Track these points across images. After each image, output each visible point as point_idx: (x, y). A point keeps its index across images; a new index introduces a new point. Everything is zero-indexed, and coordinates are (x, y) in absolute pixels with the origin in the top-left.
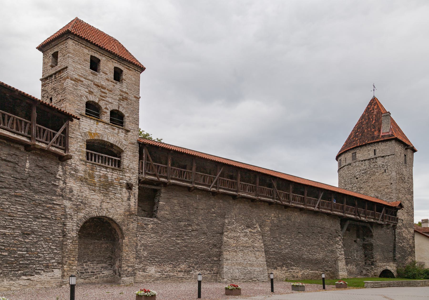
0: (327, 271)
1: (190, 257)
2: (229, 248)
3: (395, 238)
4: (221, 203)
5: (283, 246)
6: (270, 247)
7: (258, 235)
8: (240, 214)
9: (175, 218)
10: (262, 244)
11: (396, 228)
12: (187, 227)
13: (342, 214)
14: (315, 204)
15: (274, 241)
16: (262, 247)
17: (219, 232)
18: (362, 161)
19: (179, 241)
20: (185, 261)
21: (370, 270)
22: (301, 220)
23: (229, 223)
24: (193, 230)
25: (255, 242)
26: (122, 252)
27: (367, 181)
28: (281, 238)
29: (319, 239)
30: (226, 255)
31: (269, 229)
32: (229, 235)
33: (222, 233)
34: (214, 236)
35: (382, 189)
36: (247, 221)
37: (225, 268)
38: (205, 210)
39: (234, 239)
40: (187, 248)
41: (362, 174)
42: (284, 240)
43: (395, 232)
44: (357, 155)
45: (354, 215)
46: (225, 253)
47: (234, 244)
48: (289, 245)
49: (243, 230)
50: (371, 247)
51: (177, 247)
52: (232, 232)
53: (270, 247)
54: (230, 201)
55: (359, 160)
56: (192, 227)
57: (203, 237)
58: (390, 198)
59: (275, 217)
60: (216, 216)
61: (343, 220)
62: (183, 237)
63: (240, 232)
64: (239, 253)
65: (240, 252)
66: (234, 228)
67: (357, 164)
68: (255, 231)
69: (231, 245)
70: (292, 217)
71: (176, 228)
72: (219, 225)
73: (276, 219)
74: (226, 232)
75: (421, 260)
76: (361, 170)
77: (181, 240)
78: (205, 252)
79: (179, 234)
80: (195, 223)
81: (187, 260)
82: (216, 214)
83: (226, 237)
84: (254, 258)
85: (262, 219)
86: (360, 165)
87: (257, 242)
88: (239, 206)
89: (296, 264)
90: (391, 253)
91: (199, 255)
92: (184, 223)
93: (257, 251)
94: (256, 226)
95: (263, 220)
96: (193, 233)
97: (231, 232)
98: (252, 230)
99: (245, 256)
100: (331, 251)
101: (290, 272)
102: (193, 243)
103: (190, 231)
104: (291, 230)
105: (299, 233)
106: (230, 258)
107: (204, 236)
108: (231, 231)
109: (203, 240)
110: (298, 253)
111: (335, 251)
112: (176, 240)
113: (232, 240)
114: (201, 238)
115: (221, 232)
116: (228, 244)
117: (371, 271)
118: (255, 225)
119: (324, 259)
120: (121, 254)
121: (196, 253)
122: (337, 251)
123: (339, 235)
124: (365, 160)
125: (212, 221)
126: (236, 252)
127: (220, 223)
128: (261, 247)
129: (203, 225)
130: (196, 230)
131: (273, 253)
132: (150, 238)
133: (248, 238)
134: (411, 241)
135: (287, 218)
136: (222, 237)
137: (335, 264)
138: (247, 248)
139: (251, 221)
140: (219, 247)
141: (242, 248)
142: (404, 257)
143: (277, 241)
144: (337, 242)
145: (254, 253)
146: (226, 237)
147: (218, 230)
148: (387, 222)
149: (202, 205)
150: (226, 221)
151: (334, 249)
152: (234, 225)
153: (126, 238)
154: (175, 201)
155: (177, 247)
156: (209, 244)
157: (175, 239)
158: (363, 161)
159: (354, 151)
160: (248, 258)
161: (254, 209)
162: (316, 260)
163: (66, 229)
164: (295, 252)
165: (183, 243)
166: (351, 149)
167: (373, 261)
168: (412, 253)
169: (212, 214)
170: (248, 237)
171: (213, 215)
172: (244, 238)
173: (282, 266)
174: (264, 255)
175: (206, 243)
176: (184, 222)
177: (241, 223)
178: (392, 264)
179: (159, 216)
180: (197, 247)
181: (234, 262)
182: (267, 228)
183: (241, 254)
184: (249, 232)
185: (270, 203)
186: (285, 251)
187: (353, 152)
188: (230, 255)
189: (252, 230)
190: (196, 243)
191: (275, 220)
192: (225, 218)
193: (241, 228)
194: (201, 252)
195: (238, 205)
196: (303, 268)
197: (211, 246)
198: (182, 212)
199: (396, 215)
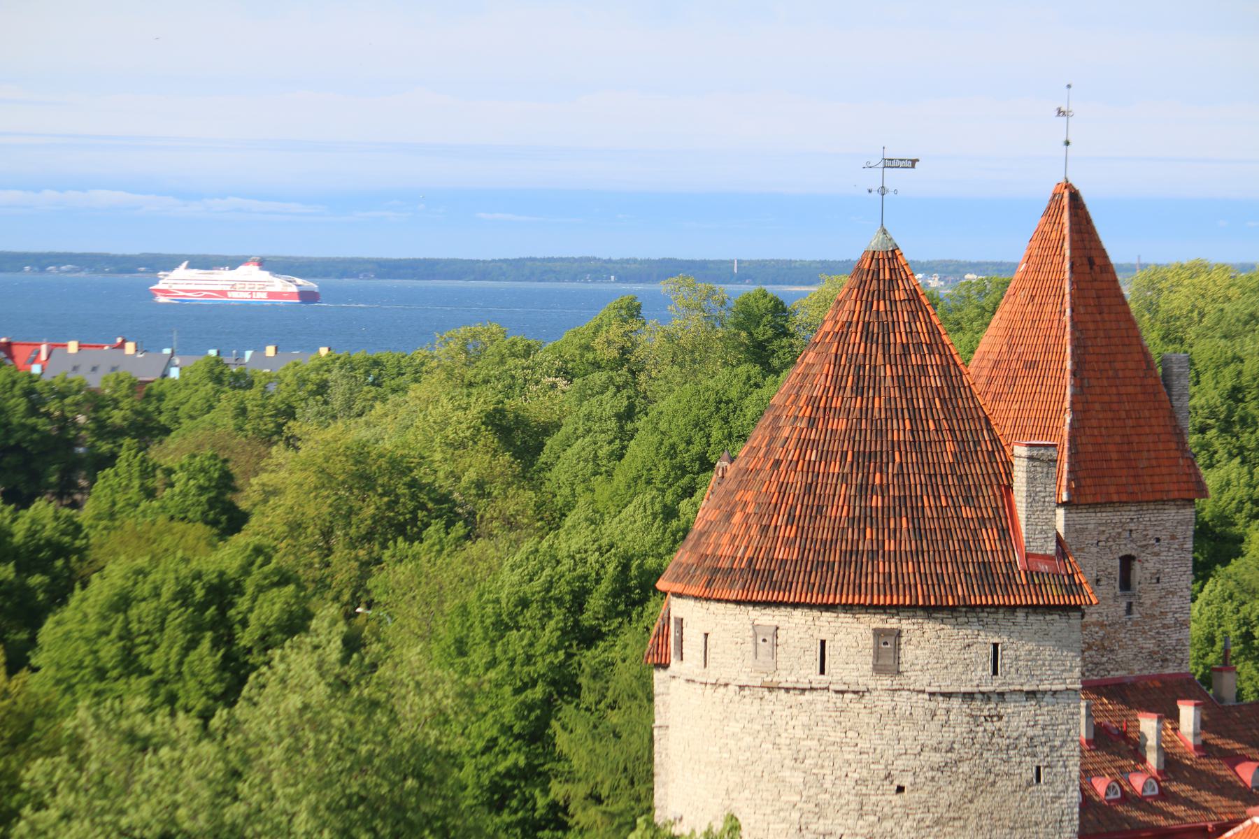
18: (932, 694)
27: (954, 819)
41: (932, 769)
44: (909, 653)
55: (918, 687)
86: (918, 713)
124: (948, 695)
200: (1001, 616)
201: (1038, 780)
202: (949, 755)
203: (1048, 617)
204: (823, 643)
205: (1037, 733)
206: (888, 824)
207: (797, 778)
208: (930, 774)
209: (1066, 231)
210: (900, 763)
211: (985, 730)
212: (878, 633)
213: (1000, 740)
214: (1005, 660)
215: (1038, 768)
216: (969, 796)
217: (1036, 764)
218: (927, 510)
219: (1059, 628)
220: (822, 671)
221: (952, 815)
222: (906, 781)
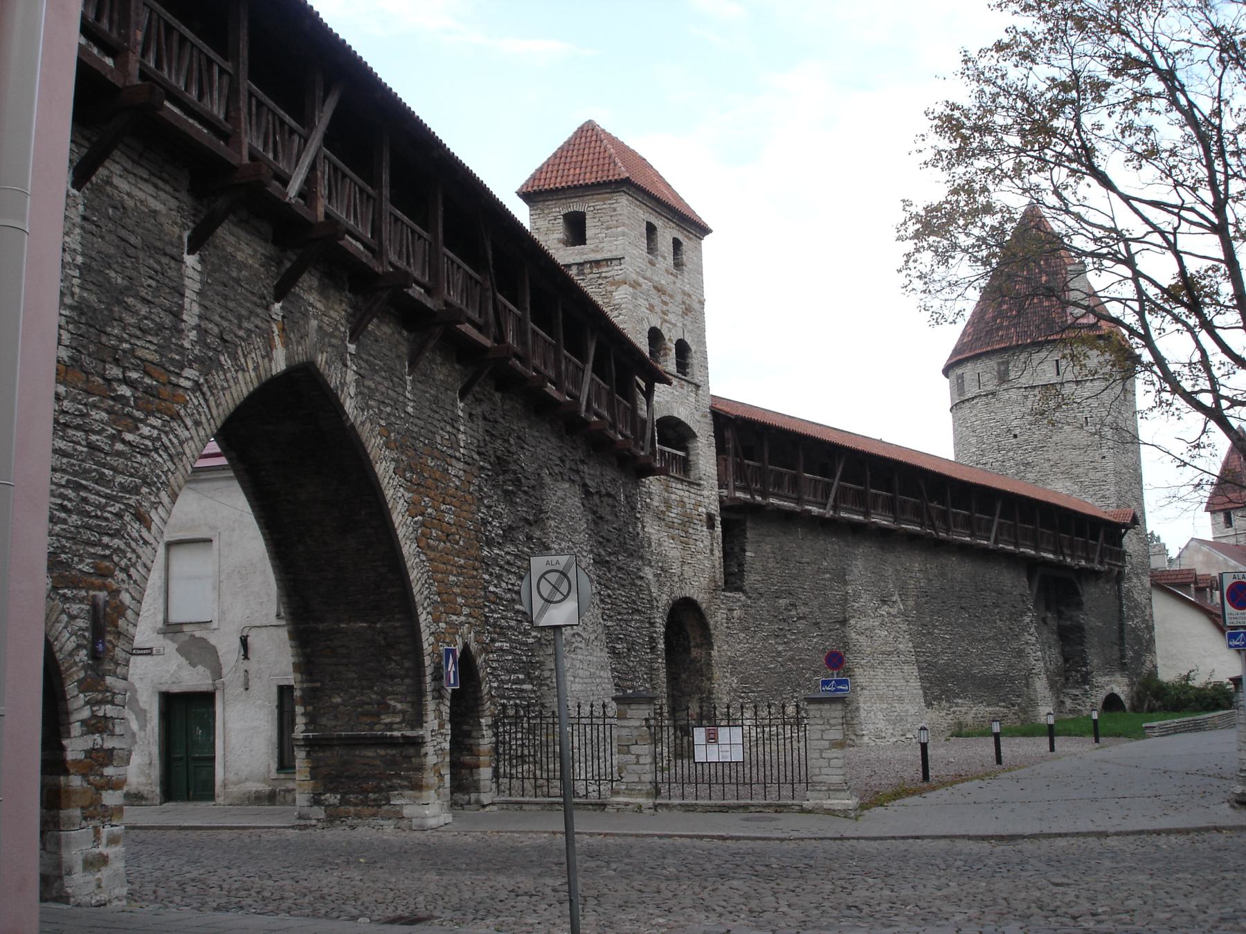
0: (1013, 705)
1: (799, 685)
3: (1121, 605)
4: (832, 545)
10: (911, 645)
11: (1122, 579)
12: (790, 610)
13: (1033, 552)
14: (989, 530)
15: (924, 635)
18: (1026, 388)
19: (780, 648)
20: (793, 697)
21: (1080, 696)
24: (799, 618)
26: (710, 679)
28: (934, 626)
30: (861, 676)
33: (844, 622)
35: (1081, 470)
37: (862, 710)
43: (1119, 590)
45: (1054, 553)
49: (876, 608)
58: (1103, 497)
59: (921, 570)
60: (830, 580)
61: (1031, 566)
68: (894, 611)
73: (922, 576)
81: (795, 695)
89: (962, 692)
90: (1116, 648)
94: (894, 599)
100: (1017, 653)
101: (954, 712)
102: (803, 649)
105: (962, 608)
115: (841, 617)
117: (1084, 699)
119: (1006, 674)
120: (706, 684)
122: (1028, 650)
123: (1029, 609)
126: (872, 667)
132: (739, 644)
134: (1147, 612)
137: (1027, 686)
142: (1138, 657)
144: (1025, 629)
148: (1109, 564)
150: (850, 589)
153: (715, 648)
154: (768, 548)
162: (994, 677)
163: (655, 632)
166: (994, 352)
167: (1087, 673)
168: (1147, 645)
169: (824, 573)
173: (938, 698)
178: (1118, 677)
179: (747, 588)
181: (873, 692)
182: (911, 603)
185: (911, 538)
192: (845, 583)
196: (977, 700)
199: (1121, 545)
206: (1011, 454)
207: (973, 440)
222: (1017, 431)
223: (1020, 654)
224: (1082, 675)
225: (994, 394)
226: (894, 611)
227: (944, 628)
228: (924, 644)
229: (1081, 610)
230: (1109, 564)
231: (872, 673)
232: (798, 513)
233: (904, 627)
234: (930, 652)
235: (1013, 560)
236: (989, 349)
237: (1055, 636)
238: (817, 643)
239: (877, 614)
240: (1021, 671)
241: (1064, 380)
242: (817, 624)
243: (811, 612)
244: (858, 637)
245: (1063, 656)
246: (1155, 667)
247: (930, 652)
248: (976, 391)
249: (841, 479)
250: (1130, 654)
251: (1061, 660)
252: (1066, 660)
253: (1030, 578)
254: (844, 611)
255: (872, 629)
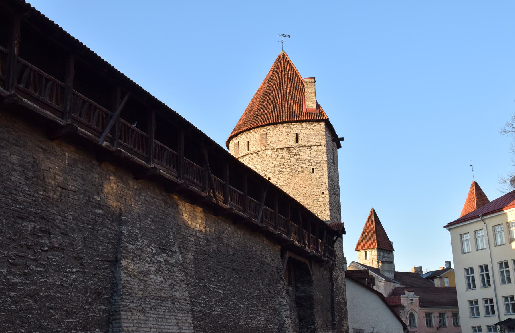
2: (131, 302)
3: (333, 286)
5: (214, 298)
6: (195, 300)
7: (178, 270)
8: (147, 217)
9: (11, 206)
10: (186, 294)
12: (38, 237)
15: (200, 287)
16: (186, 300)
17: (107, 257)
18: (277, 149)
19: (16, 280)
22: (235, 243)
23: (129, 236)
24: (52, 248)
25: (175, 287)
27: (286, 186)
29: (259, 285)
31: (192, 257)
32: (131, 267)
33: (115, 262)
34: (96, 268)
36: (159, 236)
38: (80, 194)
39: (140, 279)
40: (36, 301)
42: (214, 285)
43: (331, 277)
44: (269, 139)
46: (125, 315)
47: (141, 293)
48: (222, 296)
49: (154, 255)
50: (309, 302)
51: (10, 297)
52: (135, 259)
53: (195, 300)
54: (130, 182)
55: (273, 148)
56: (49, 238)
57: (74, 270)
62: (27, 266)
63: (149, 260)
64: (149, 315)
65: (150, 312)
66: (139, 249)
67: (269, 155)
69: (134, 295)
70: (224, 235)
71: (10, 238)
72: (108, 238)
74: (125, 258)
75: (356, 326)
76: (275, 165)
77: (20, 275)
78: (77, 314)
79: (17, 255)
80: (58, 227)
82: (103, 210)
83: (125, 273)
84: (175, 327)
85: (182, 233)
86: (273, 155)
87: (178, 288)
88: (145, 196)
90: (330, 314)
91: (63, 322)
92: (33, 224)
93: (179, 310)
95: (184, 237)
96: (53, 255)
97: (133, 260)
98: (169, 259)
99: (159, 324)
103: (47, 248)
104: (224, 263)
106: (134, 329)
107: (76, 267)
108: (134, 257)
109: (74, 276)
110: (234, 315)
111: (278, 310)
112: (10, 273)
113: (136, 280)
114: (70, 272)
116: (130, 291)
118: (173, 246)
121: (56, 317)
123: (282, 279)
124: (282, 149)
125: (95, 226)
126: (143, 311)
127: (111, 233)
128: (184, 299)
129: (75, 236)
130: (61, 249)
131: (199, 315)
133: (163, 277)
134: (344, 292)
135: (218, 236)
136: (113, 272)
138: (163, 301)
139: (167, 237)
140: (106, 298)
141: (154, 301)
143: (205, 286)
144: (279, 293)
145: (175, 316)
146: (126, 271)
147: (106, 253)
149: (76, 181)
151: (276, 305)
152: (138, 243)
155: (10, 297)
156: (85, 290)
157: (5, 271)
158: (279, 150)
159: (263, 131)
160: (166, 327)
161: (170, 210)
164: (229, 312)
165: (25, 283)
168: (344, 314)
169: (95, 208)
170: (163, 275)
171: (97, 211)
172: (157, 276)
174: (190, 319)
175: (81, 286)
176: (33, 222)
177: (150, 239)
180: (59, 297)
182: (190, 256)
183: (154, 318)
184: (164, 263)
186: (216, 311)
187: (260, 131)
188: (133, 320)
189: (169, 259)
190: (58, 286)
191: (201, 239)
193: (150, 250)
194: (69, 314)
195: (143, 194)
197: (90, 296)
198: (29, 191)
199: (333, 247)
200: (297, 125)
201: (313, 172)
202: (283, 167)
203: (313, 125)
204: (248, 142)
205: (311, 158)
208: (277, 173)
209: (474, 189)
210: (269, 171)
211: (294, 159)
212: (261, 135)
213: (299, 161)
214: (300, 138)
215: (313, 169)
216: (290, 178)
217: (312, 168)
218: (279, 102)
219: (317, 128)
220: (248, 150)
221: (285, 184)
223: (276, 311)
224: (311, 331)
225: (257, 152)
226: (173, 261)
227: (218, 284)
228: (200, 295)
229: (312, 286)
230: (328, 257)
231: (142, 318)
232: (62, 127)
233: (182, 276)
234: (205, 303)
235: (275, 239)
236: (255, 125)
237: (294, 304)
238: (75, 280)
239: (153, 260)
240: (275, 325)
241: (301, 145)
242: (78, 258)
243: (72, 245)
244: (129, 279)
245: (298, 317)
246: (348, 328)
247: (205, 303)
248: (246, 152)
249: (122, 115)
250: (337, 318)
251: (297, 320)
252: (300, 321)
253: (282, 256)
254: (117, 251)
255: (146, 273)
